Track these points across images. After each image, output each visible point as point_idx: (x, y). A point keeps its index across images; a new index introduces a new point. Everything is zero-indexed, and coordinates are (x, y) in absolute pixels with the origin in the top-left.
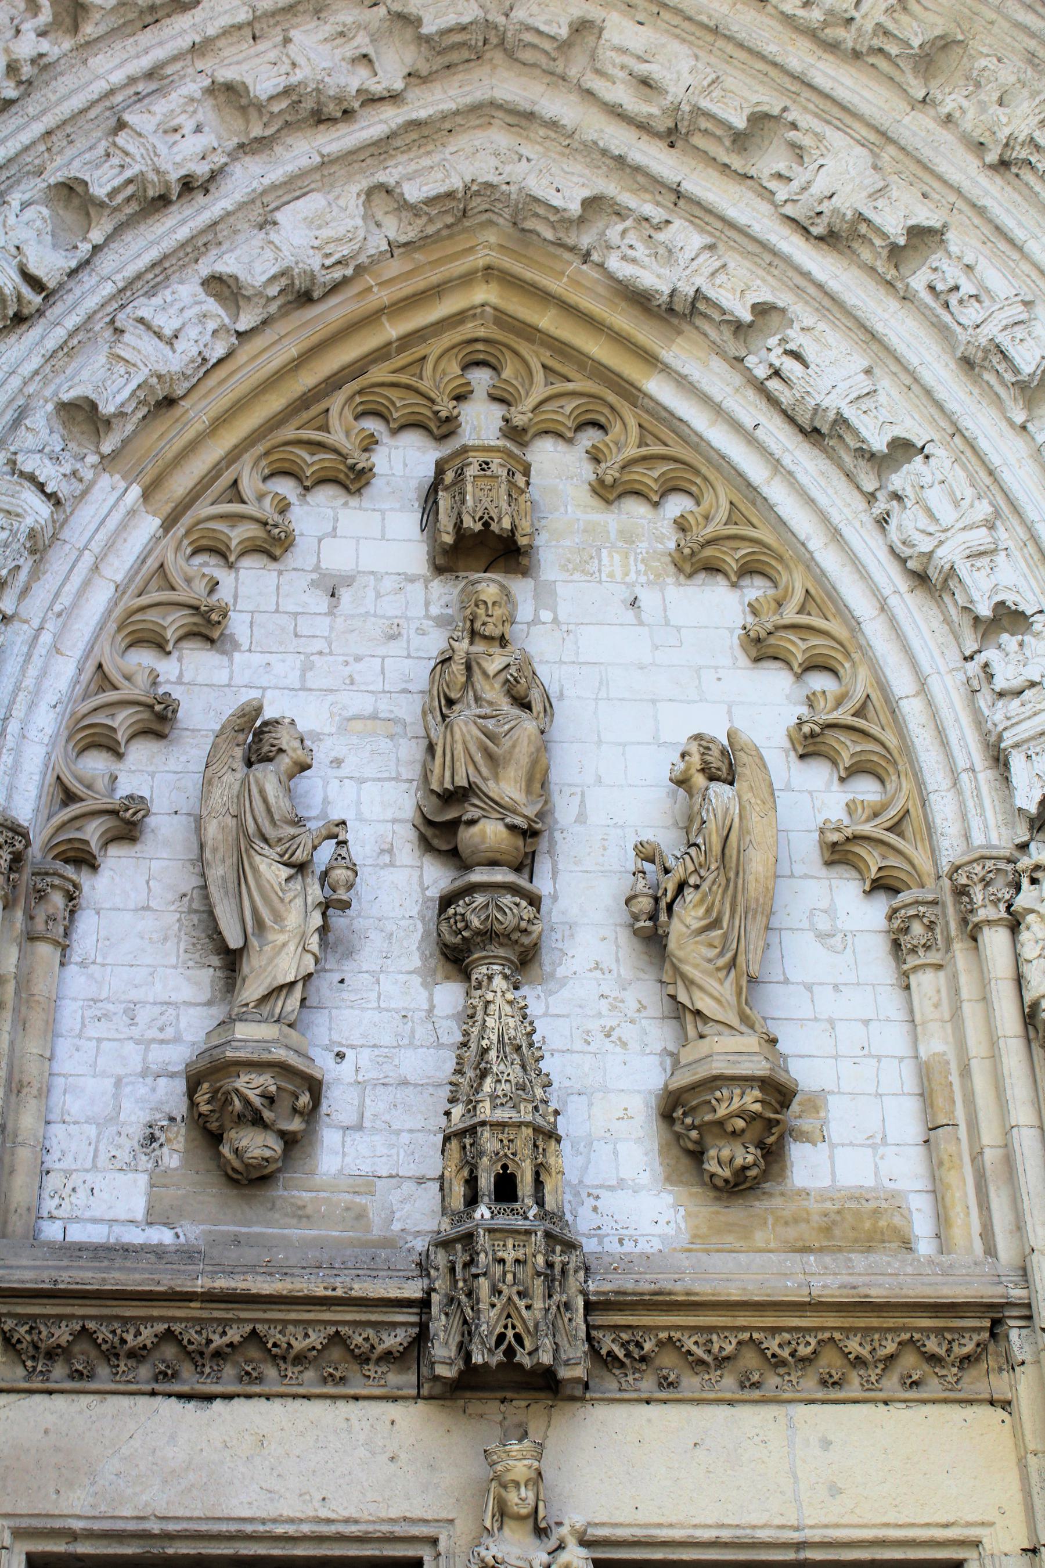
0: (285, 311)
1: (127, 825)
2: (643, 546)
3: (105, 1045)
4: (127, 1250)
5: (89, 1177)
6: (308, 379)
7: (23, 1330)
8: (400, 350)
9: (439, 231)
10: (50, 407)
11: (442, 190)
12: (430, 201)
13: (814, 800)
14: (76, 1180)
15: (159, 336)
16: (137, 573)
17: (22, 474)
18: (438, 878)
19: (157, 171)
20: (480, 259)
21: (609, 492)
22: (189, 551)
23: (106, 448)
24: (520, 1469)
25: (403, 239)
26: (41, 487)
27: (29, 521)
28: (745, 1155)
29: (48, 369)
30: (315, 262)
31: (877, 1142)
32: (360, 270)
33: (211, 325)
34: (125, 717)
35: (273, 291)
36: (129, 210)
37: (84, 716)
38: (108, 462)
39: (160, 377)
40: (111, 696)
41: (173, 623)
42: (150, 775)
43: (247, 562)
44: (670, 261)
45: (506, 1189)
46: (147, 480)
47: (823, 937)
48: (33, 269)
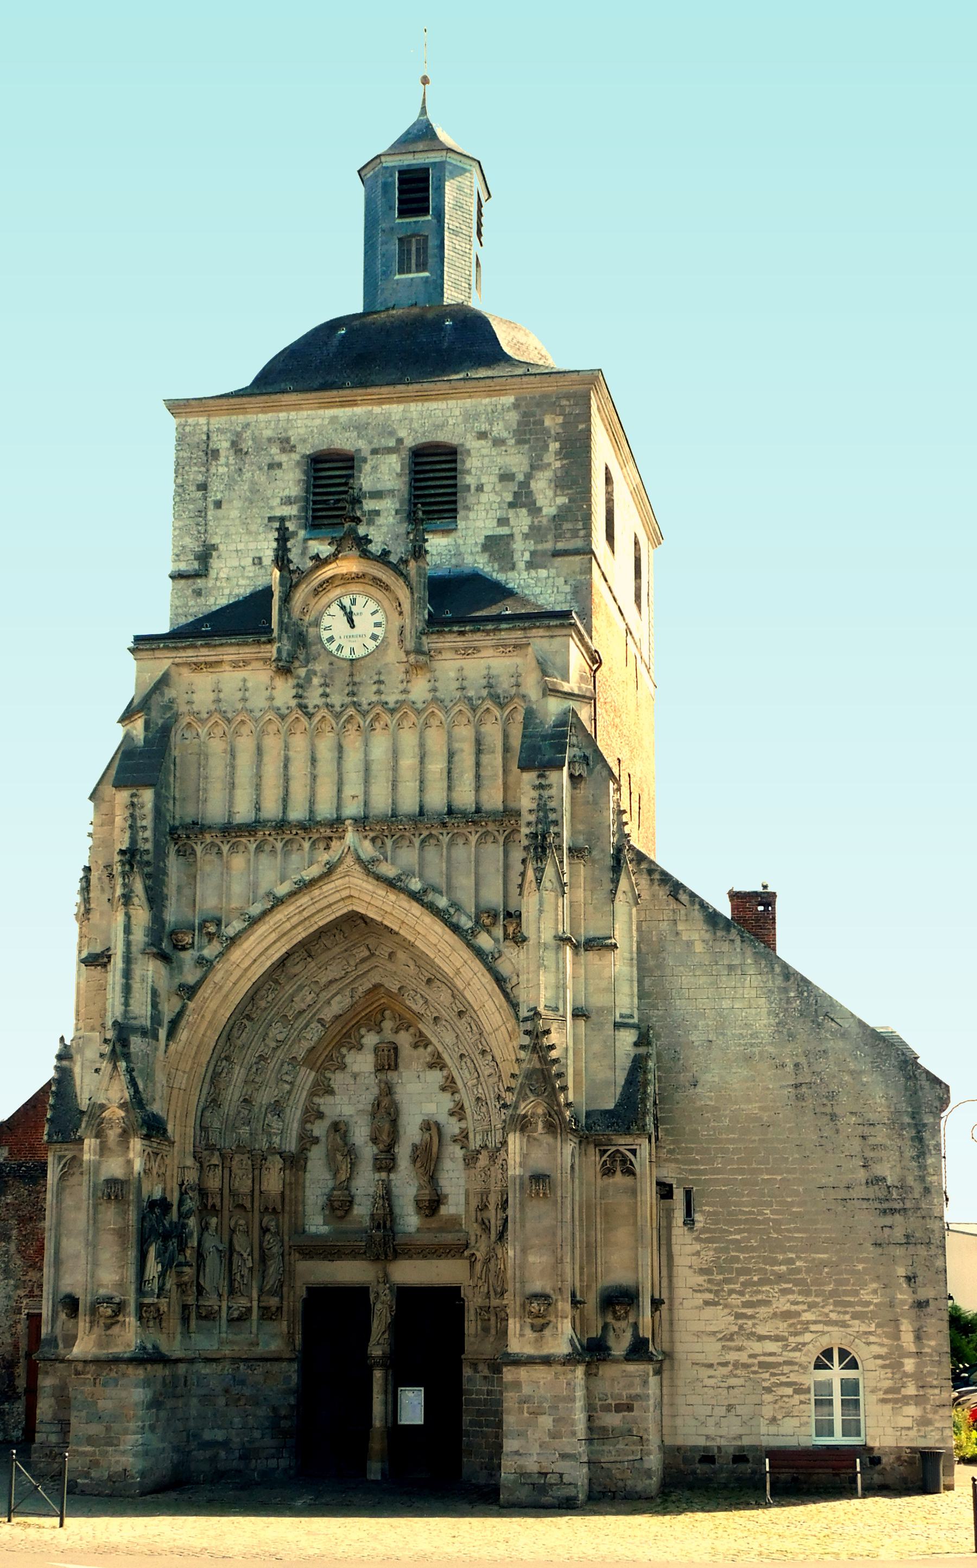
2: (421, 1061)
21: (416, 1046)
47: (451, 1159)
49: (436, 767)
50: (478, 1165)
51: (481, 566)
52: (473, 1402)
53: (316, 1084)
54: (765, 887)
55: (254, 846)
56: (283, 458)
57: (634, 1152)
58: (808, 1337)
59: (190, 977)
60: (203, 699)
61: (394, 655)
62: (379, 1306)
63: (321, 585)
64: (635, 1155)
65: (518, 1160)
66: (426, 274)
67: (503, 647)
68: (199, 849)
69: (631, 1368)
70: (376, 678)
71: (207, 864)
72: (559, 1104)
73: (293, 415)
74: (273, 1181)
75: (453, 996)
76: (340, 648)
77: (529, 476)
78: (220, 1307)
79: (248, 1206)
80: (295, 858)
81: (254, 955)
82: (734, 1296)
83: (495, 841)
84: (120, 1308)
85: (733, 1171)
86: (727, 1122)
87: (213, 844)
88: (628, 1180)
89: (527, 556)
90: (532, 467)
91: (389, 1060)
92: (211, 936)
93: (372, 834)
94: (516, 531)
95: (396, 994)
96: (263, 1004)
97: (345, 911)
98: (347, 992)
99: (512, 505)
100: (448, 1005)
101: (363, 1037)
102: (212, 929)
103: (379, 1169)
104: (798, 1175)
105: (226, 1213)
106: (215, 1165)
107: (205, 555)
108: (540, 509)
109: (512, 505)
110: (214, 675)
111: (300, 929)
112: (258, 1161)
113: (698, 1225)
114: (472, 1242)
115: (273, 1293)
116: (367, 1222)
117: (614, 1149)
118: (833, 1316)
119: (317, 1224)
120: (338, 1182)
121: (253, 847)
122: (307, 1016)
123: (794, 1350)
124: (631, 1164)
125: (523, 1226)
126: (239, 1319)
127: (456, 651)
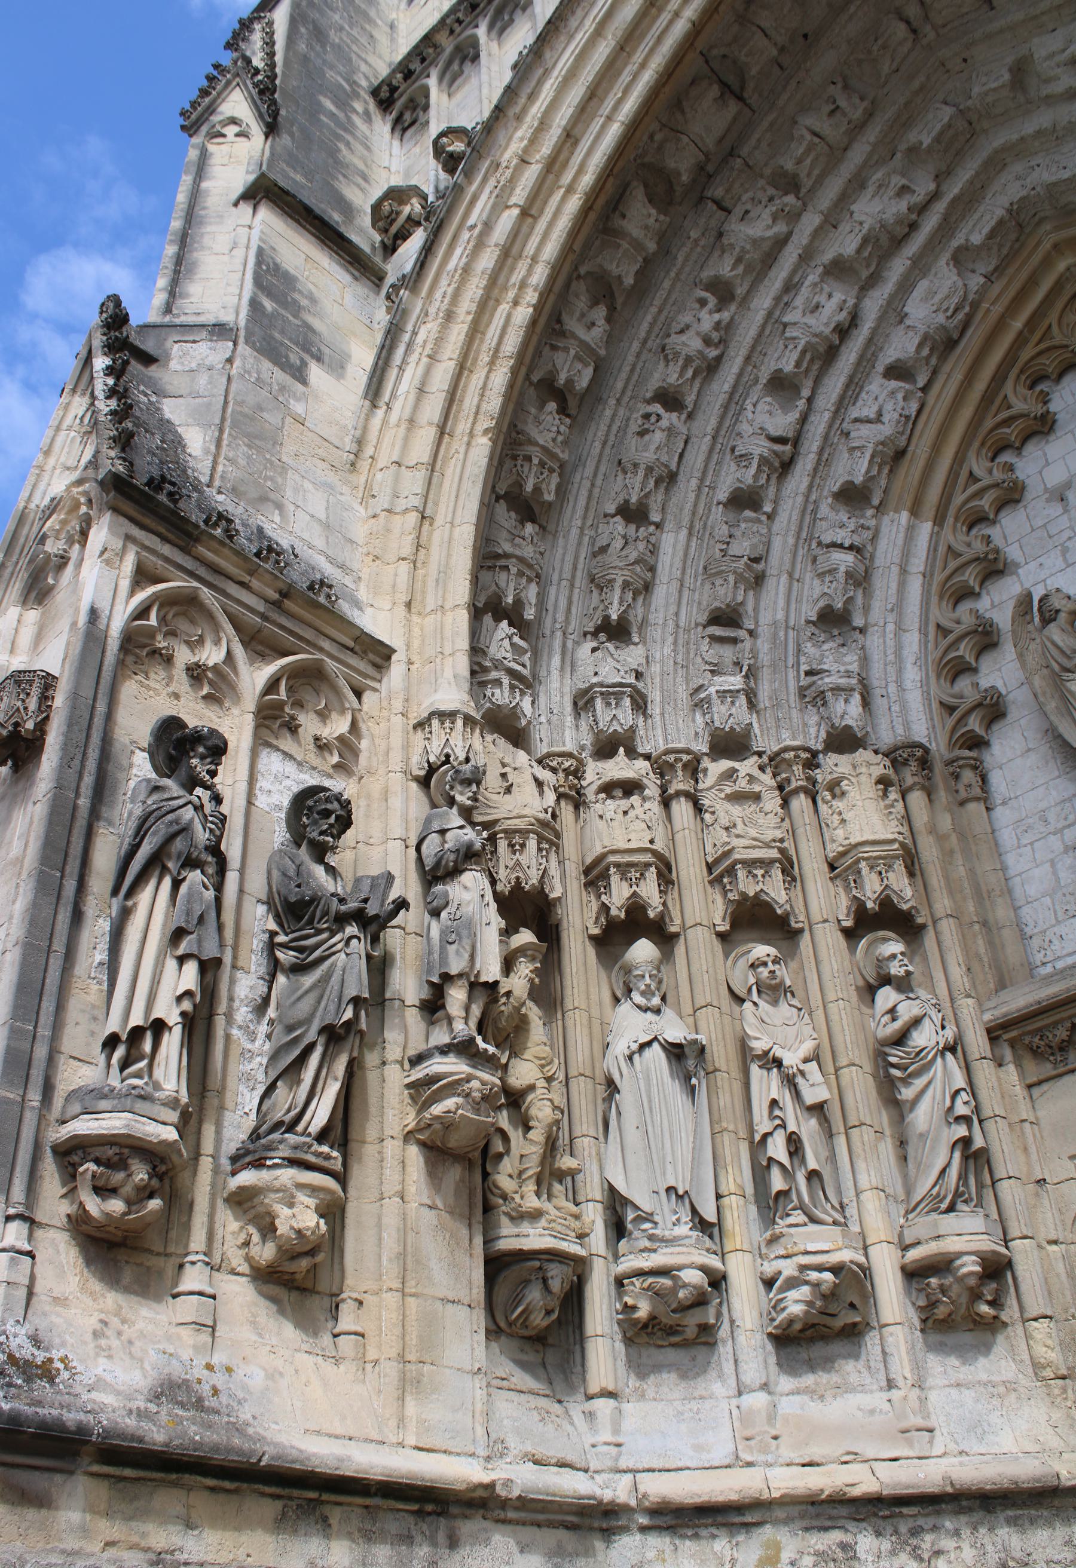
0: (943, 357)
1: (994, 710)
3: (1036, 844)
5: (1055, 929)
6: (980, 386)
7: (1036, 1039)
8: (1032, 332)
9: (1011, 248)
10: (830, 500)
11: (993, 223)
12: (991, 235)
14: (1049, 935)
15: (869, 421)
16: (934, 559)
17: (828, 546)
19: (816, 335)
20: (1047, 245)
22: (964, 529)
23: (876, 502)
25: (991, 268)
26: (841, 546)
27: (842, 569)
29: (817, 480)
30: (941, 318)
32: (975, 305)
33: (900, 396)
35: (926, 352)
36: (816, 367)
37: (941, 659)
38: (880, 509)
39: (882, 443)
40: (951, 638)
41: (970, 577)
43: (1002, 514)
46: (909, 504)
48: (775, 433)
78: (717, 1281)
96: (692, 343)
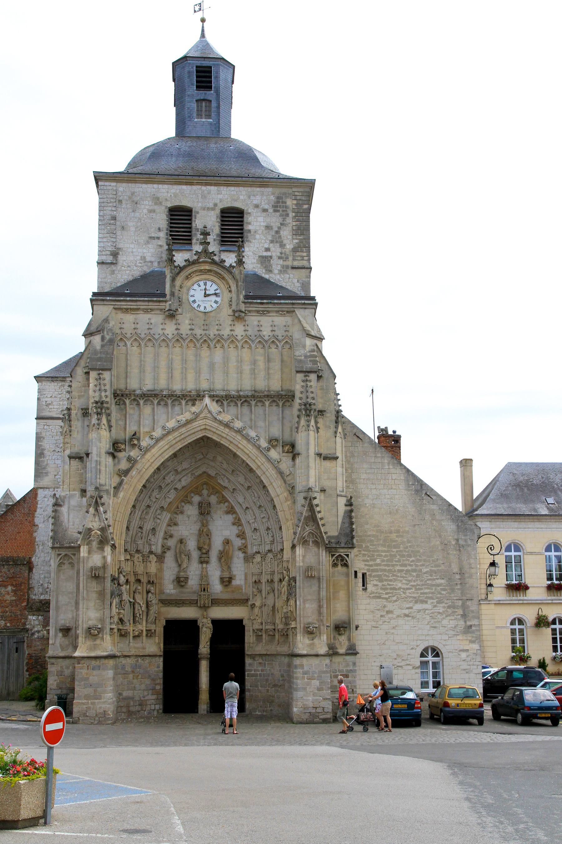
1: (169, 549)
4: (172, 595)
13: (238, 542)
18: (199, 553)
24: (205, 614)
28: (227, 583)
31: (240, 580)
34: (168, 536)
42: (171, 543)
44: (225, 483)
45: (204, 590)
49: (247, 368)
50: (255, 560)
51: (256, 270)
52: (253, 675)
53: (171, 519)
54: (394, 432)
55: (157, 401)
56: (156, 207)
57: (347, 555)
58: (419, 642)
59: (124, 465)
60: (128, 328)
61: (227, 312)
62: (204, 629)
63: (190, 274)
64: (348, 557)
65: (301, 558)
66: (211, 120)
67: (280, 313)
68: (127, 402)
69: (348, 658)
70: (217, 322)
71: (131, 409)
72: (321, 532)
73: (160, 186)
74: (153, 568)
75: (245, 479)
76: (199, 306)
77: (279, 228)
79: (142, 580)
80: (177, 408)
81: (157, 456)
82: (386, 623)
83: (278, 405)
84: (100, 630)
85: (384, 565)
86: (381, 542)
87: (134, 400)
88: (344, 569)
89: (279, 267)
90: (281, 224)
91: (205, 511)
92: (134, 445)
93: (217, 399)
94: (274, 254)
95: (213, 477)
97: (201, 435)
98: (189, 475)
99: (272, 242)
100: (242, 483)
101: (193, 497)
102: (136, 442)
103: (202, 563)
104: (414, 567)
105: (132, 583)
106: (128, 560)
107: (115, 254)
108: (285, 245)
109: (272, 242)
110: (134, 316)
111: (179, 444)
112: (145, 559)
113: (368, 590)
114: (251, 597)
115: (151, 623)
116: (196, 588)
117: (338, 554)
118: (430, 633)
119: (170, 589)
120: (182, 569)
121: (156, 402)
122: (170, 487)
123: (412, 649)
124: (346, 561)
125: (303, 591)
126: (138, 636)
127: (258, 312)
